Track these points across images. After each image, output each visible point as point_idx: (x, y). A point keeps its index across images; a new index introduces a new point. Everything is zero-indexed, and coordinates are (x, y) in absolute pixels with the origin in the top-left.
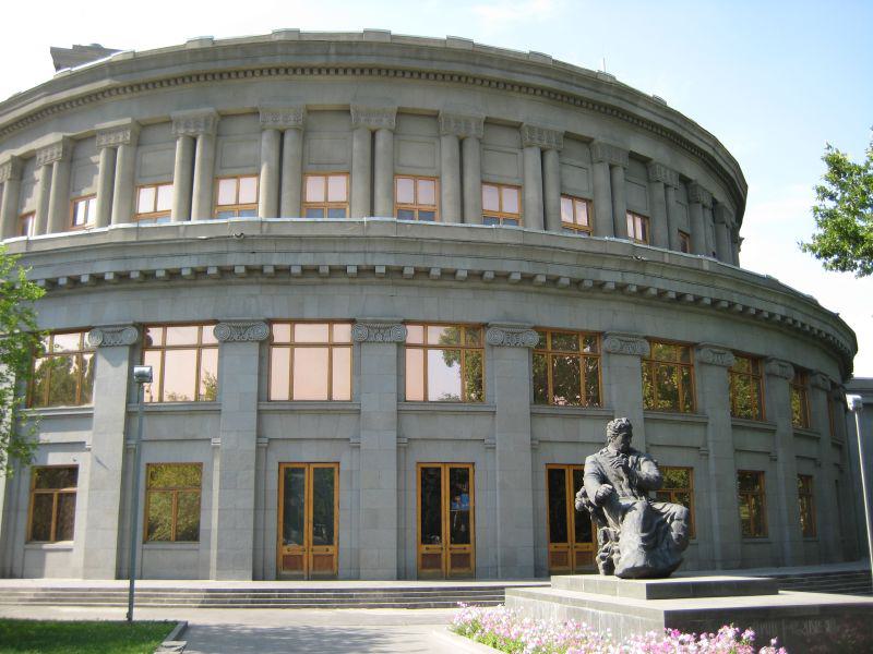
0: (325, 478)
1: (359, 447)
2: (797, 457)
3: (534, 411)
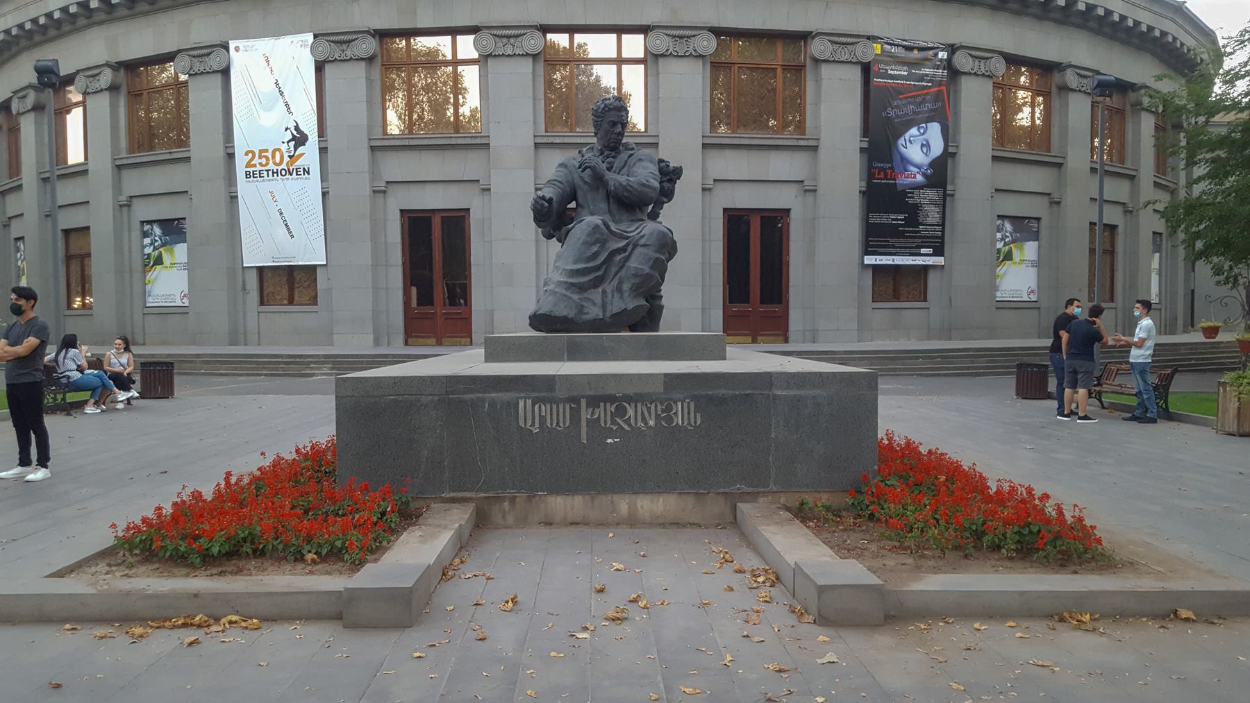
0: (456, 222)
1: (489, 190)
2: (1091, 199)
3: (707, 141)
